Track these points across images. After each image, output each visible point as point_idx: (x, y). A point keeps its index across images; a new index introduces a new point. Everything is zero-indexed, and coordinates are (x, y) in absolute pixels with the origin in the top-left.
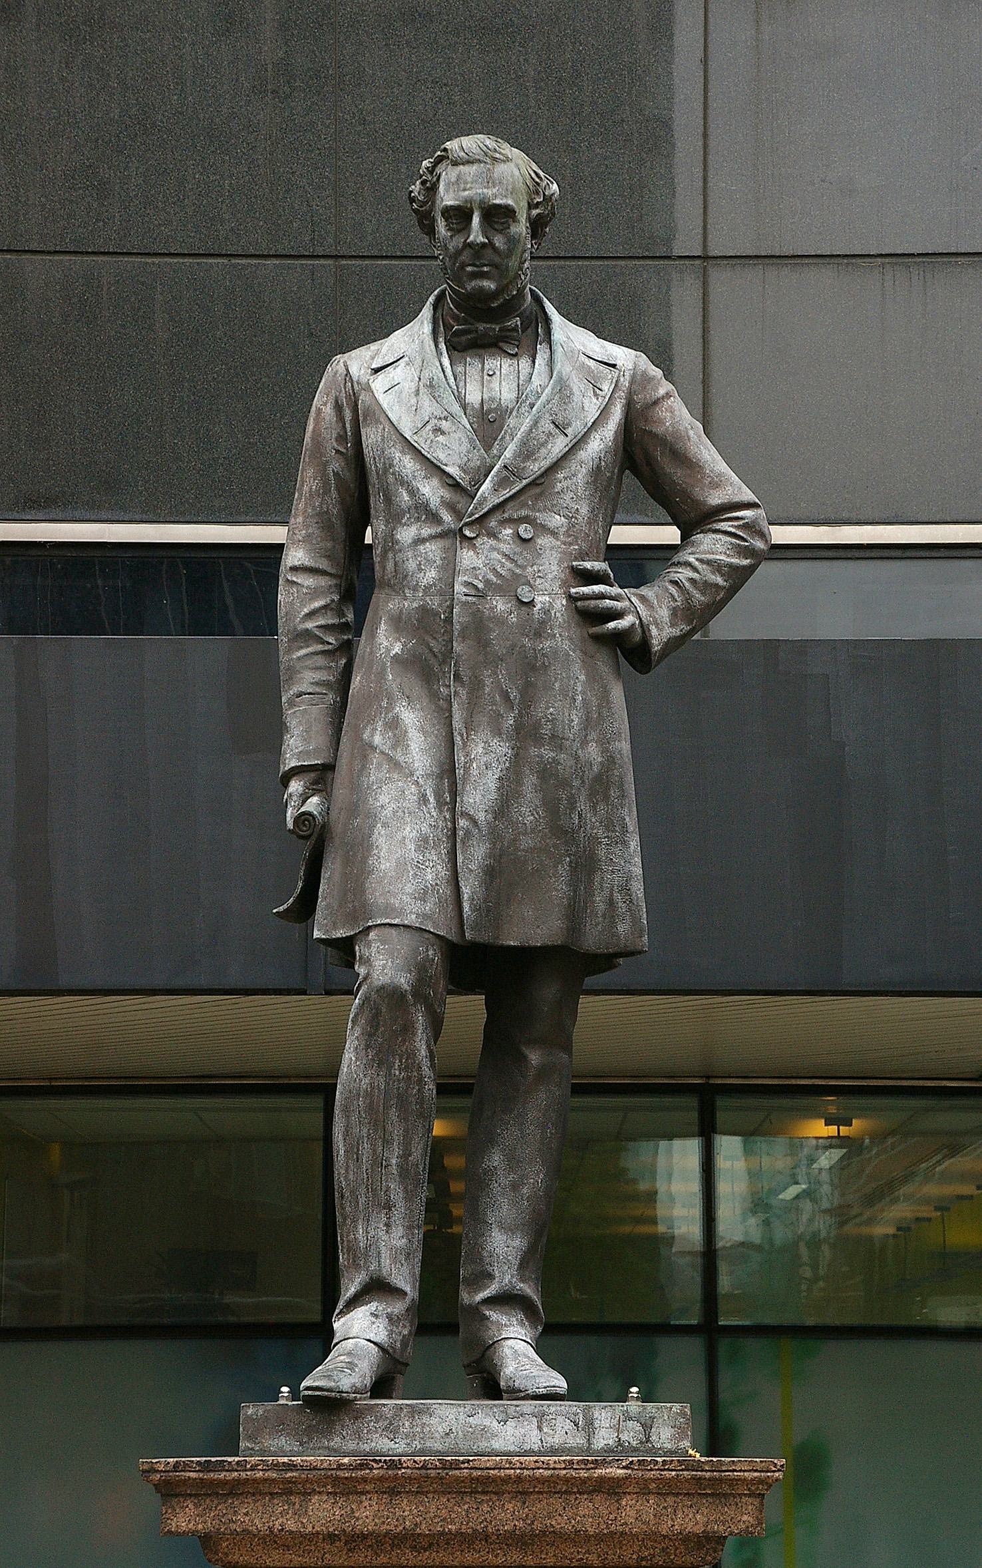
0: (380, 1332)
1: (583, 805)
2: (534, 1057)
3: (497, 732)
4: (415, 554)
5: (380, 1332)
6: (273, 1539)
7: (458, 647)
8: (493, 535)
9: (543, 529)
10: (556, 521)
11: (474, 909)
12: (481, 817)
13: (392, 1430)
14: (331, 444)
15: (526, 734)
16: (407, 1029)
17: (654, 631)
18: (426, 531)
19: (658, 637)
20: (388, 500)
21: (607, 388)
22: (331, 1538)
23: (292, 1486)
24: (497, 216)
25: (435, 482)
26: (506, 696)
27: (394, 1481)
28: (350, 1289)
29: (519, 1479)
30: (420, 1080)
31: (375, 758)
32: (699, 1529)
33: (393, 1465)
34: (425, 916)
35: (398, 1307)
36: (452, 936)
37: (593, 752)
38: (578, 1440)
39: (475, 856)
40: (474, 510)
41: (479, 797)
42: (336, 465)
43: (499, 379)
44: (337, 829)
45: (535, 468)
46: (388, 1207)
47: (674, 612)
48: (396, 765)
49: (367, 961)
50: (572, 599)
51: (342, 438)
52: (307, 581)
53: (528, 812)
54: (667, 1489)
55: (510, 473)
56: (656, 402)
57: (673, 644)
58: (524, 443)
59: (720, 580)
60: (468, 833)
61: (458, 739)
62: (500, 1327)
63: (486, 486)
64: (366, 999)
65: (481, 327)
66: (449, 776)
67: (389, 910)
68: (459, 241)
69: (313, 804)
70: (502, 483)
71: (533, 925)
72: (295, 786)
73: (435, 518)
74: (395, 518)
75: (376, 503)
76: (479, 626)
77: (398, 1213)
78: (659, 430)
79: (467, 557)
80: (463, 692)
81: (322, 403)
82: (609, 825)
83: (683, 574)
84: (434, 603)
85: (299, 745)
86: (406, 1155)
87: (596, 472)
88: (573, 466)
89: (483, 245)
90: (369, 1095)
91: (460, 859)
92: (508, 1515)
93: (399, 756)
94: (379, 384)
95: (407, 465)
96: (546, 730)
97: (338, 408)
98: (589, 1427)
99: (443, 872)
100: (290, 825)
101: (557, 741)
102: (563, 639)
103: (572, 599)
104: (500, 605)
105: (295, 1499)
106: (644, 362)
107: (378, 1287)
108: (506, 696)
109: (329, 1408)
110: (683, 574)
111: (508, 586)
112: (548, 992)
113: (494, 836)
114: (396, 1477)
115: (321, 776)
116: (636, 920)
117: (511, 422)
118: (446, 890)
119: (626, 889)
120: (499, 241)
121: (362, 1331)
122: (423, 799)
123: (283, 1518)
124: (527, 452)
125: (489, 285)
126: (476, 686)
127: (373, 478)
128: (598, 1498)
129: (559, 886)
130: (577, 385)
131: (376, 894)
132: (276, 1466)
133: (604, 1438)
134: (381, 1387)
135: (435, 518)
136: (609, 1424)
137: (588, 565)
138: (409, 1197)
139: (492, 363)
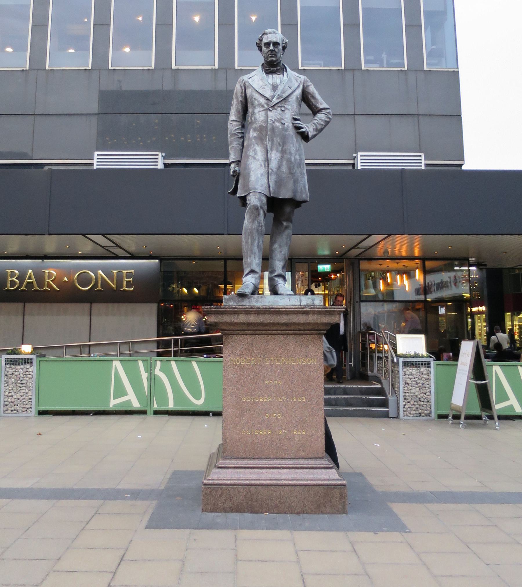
0: (253, 281)
1: (296, 168)
2: (285, 224)
3: (277, 151)
4: (258, 115)
5: (253, 281)
6: (231, 324)
7: (269, 133)
8: (276, 109)
9: (286, 109)
10: (289, 107)
11: (273, 189)
12: (274, 170)
13: (257, 301)
14: (239, 94)
15: (283, 152)
16: (259, 215)
17: (309, 133)
18: (261, 109)
19: (310, 134)
20: (252, 104)
21: (299, 81)
22: (244, 324)
23: (235, 312)
24: (276, 44)
25: (263, 99)
26: (279, 144)
27: (259, 312)
28: (246, 271)
29: (286, 311)
30: (261, 226)
31: (250, 158)
32: (326, 322)
33: (258, 308)
34: (263, 190)
35: (257, 276)
36: (268, 195)
37: (298, 157)
38: (298, 303)
39: (272, 178)
40: (272, 104)
41: (273, 165)
42: (240, 99)
43: (276, 78)
44: (242, 172)
45: (285, 95)
46: (255, 254)
47: (314, 129)
48: (255, 158)
49: (250, 200)
50: (293, 124)
51: (242, 93)
52: (235, 123)
53: (284, 169)
54: (319, 313)
55: (279, 96)
56: (309, 86)
57: (314, 136)
58: (283, 90)
59: (323, 123)
60: (271, 173)
61: (269, 153)
62: (278, 281)
63: (274, 99)
64: (250, 208)
65: (272, 69)
66: (267, 160)
67: (255, 189)
68: (268, 50)
69: (237, 168)
70: (278, 98)
71: (285, 194)
72: (233, 165)
73: (263, 106)
74: (254, 107)
75: (250, 105)
76: (273, 129)
77: (257, 255)
78: (310, 91)
79: (270, 114)
80: (270, 143)
81: (238, 86)
82: (301, 173)
83: (315, 122)
84: (263, 124)
85: (233, 157)
86: (259, 242)
87: (297, 98)
88: (292, 96)
89: (273, 50)
90: (250, 229)
91: (270, 178)
92: (284, 319)
93: (256, 157)
94: (250, 81)
95: (257, 96)
96: (288, 151)
97: (241, 87)
98: (300, 300)
99: (266, 181)
100: (231, 173)
101: (290, 153)
102: (291, 132)
103: (293, 124)
104: (278, 124)
105: (236, 315)
106: (306, 78)
107: (252, 271)
108: (279, 144)
109: (242, 296)
110: (315, 122)
111: (279, 120)
112: (288, 209)
113: (277, 174)
114: (259, 311)
115: (238, 163)
116: (306, 195)
117: (279, 87)
118: (267, 185)
119: (304, 187)
120: (276, 50)
121: (249, 281)
122: (261, 166)
123: (233, 319)
124: (283, 92)
125: (274, 59)
126: (273, 141)
127: (249, 100)
128: (304, 315)
129: (291, 185)
130: (293, 80)
131: (251, 186)
132: (232, 308)
133: (304, 303)
134: (253, 293)
135: (263, 106)
136: (305, 301)
137: (296, 117)
138: (259, 252)
139: (274, 76)
